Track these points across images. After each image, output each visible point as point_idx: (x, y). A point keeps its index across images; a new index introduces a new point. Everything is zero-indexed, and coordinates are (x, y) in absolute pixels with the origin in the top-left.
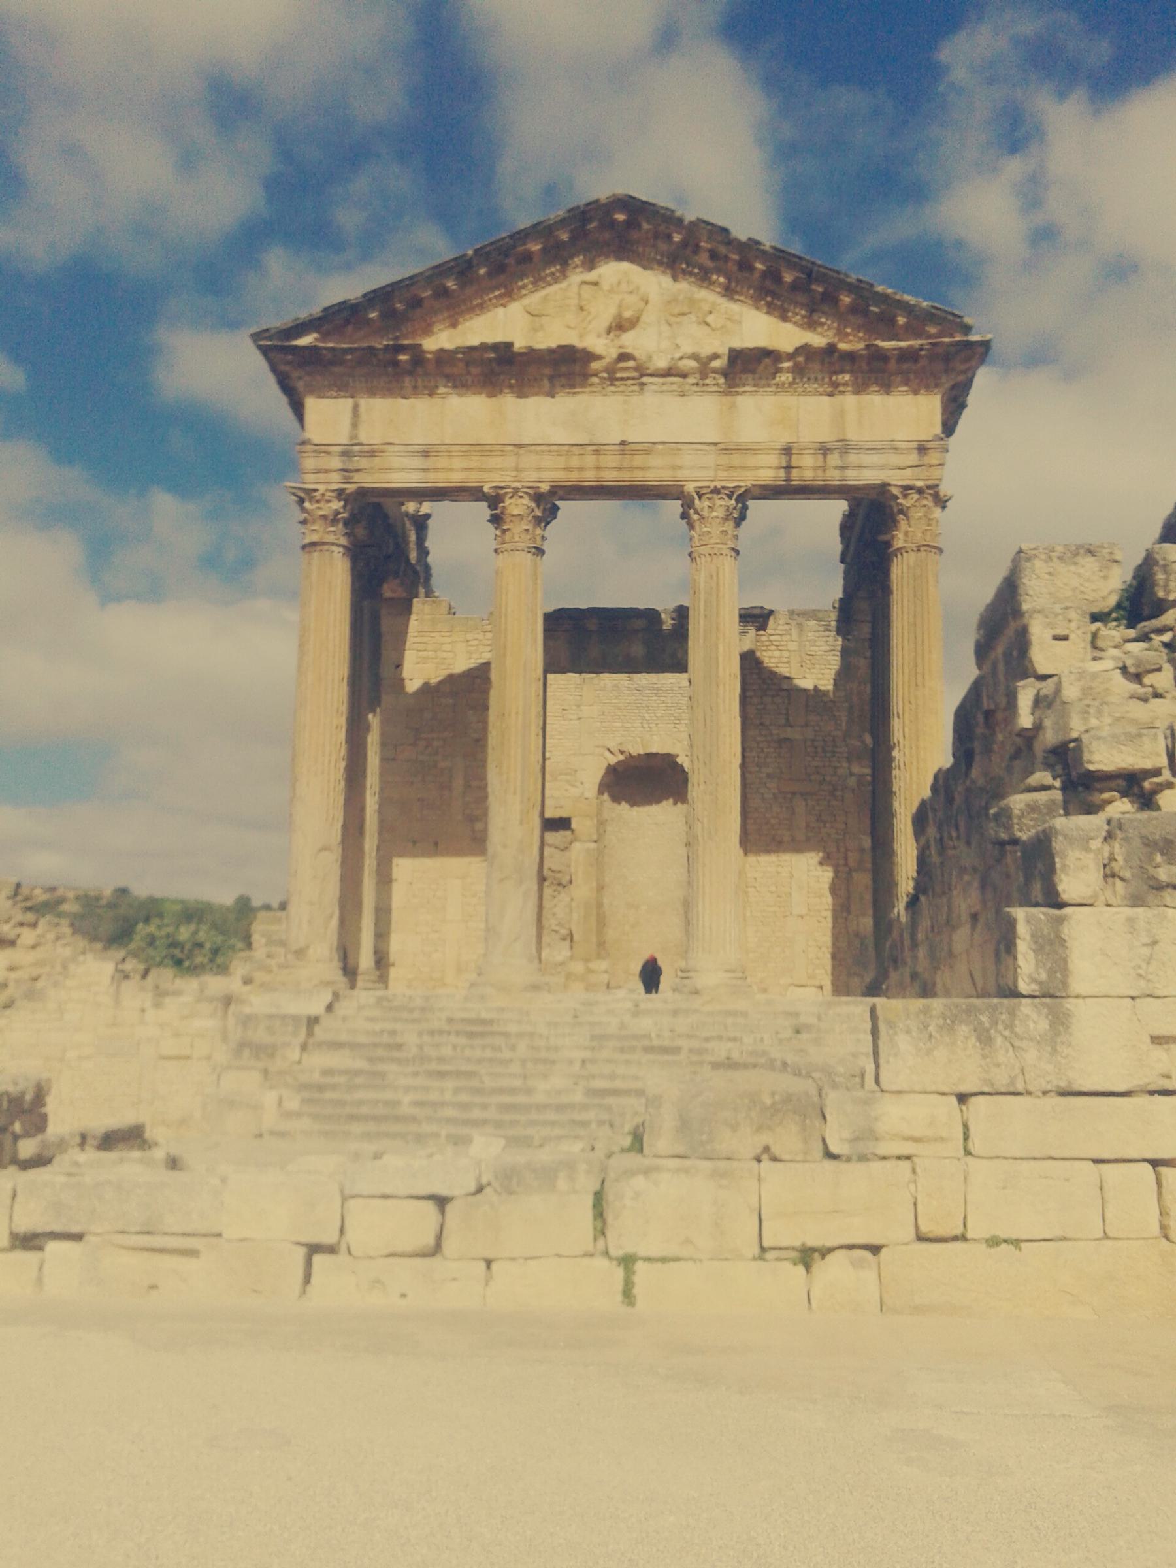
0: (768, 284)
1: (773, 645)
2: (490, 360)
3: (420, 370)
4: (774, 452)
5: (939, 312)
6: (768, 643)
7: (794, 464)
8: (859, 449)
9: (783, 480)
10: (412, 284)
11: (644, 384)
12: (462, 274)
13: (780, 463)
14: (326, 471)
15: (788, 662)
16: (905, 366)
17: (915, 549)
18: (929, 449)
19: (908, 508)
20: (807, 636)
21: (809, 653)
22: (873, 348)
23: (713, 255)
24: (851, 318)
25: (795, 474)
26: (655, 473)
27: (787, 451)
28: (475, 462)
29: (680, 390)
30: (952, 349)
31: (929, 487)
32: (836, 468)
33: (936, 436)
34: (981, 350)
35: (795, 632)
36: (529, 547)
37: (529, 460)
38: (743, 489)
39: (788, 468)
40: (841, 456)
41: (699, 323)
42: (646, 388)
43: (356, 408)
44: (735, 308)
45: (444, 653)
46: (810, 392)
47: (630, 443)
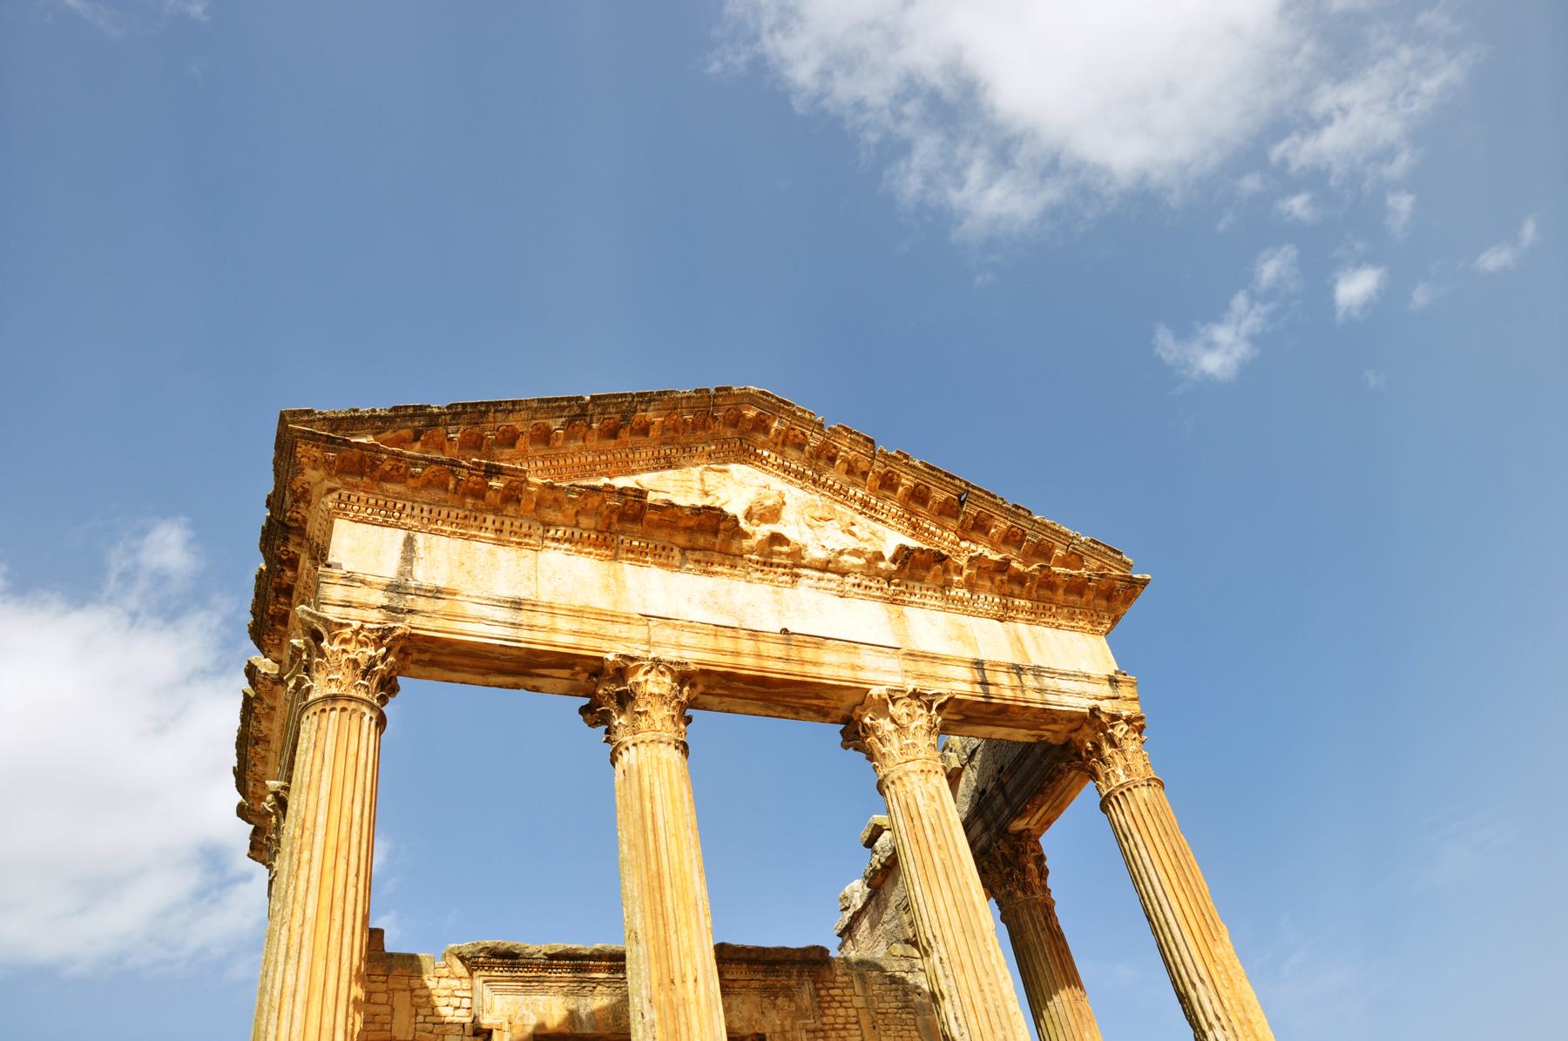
0: (911, 503)
1: (835, 1001)
2: (612, 510)
3: (511, 509)
4: (964, 664)
5: (1099, 547)
6: (828, 999)
7: (990, 680)
9: (983, 697)
10: (511, 412)
11: (798, 576)
12: (571, 421)
13: (974, 676)
14: (363, 606)
15: (857, 1023)
16: (1071, 598)
17: (1145, 783)
18: (1117, 681)
19: (1120, 740)
20: (873, 990)
21: (879, 1011)
22: (1045, 572)
25: (993, 690)
26: (830, 668)
27: (978, 665)
28: (589, 626)
29: (838, 588)
35: (857, 985)
36: (676, 741)
37: (661, 633)
38: (946, 698)
39: (984, 683)
40: (1036, 679)
41: (843, 531)
42: (800, 580)
43: (409, 543)
44: (878, 526)
45: (376, 1007)
46: (981, 613)
47: (793, 634)
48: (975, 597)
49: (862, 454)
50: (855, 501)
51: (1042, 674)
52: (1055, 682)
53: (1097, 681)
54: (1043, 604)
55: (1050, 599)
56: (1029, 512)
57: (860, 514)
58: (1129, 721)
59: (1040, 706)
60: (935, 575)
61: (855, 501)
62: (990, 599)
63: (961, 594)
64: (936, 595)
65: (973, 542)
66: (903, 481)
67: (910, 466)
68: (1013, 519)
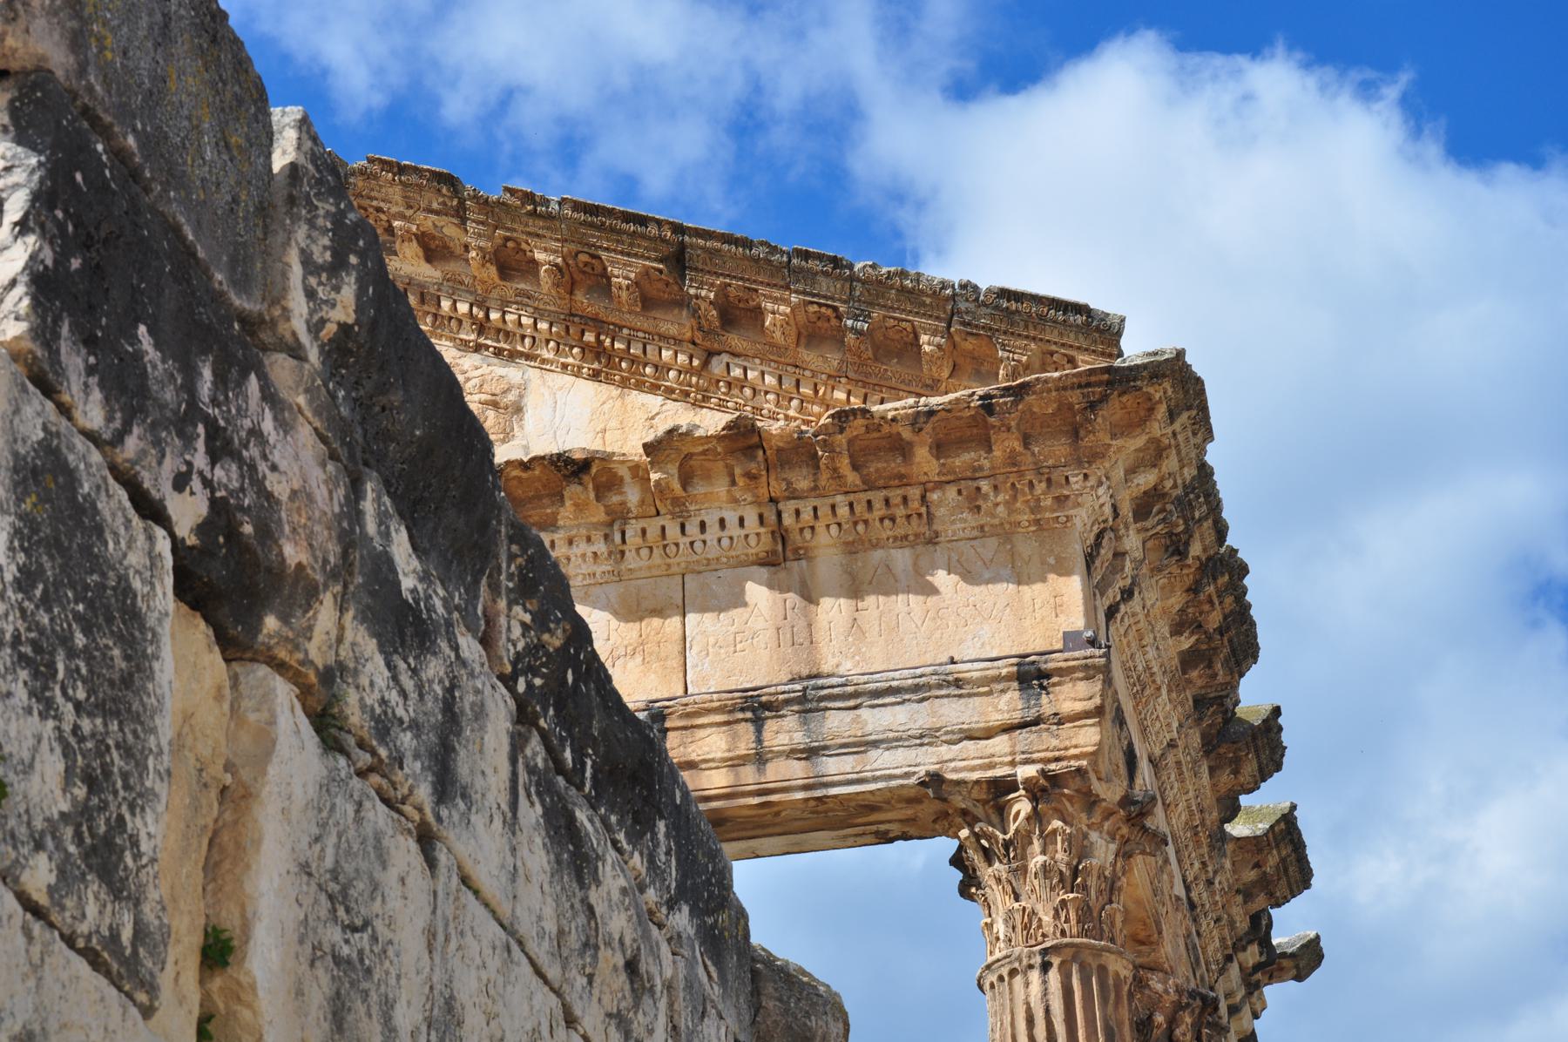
0: (580, 297)
5: (1024, 307)
8: (857, 696)
16: (962, 460)
17: (1038, 960)
18: (1048, 675)
19: (1007, 845)
23: (433, 250)
24: (808, 356)
30: (1075, 397)
31: (1054, 780)
32: (792, 753)
33: (1067, 636)
34: (1161, 391)
40: (805, 723)
44: (513, 373)
48: (692, 528)
49: (437, 213)
50: (460, 322)
51: (822, 704)
52: (856, 720)
53: (990, 685)
54: (884, 493)
55: (901, 477)
56: (835, 261)
57: (478, 348)
58: (1036, 792)
59: (800, 795)
60: (576, 505)
61: (460, 322)
62: (731, 517)
63: (654, 532)
64: (594, 548)
65: (734, 355)
66: (540, 256)
67: (541, 216)
68: (800, 287)
